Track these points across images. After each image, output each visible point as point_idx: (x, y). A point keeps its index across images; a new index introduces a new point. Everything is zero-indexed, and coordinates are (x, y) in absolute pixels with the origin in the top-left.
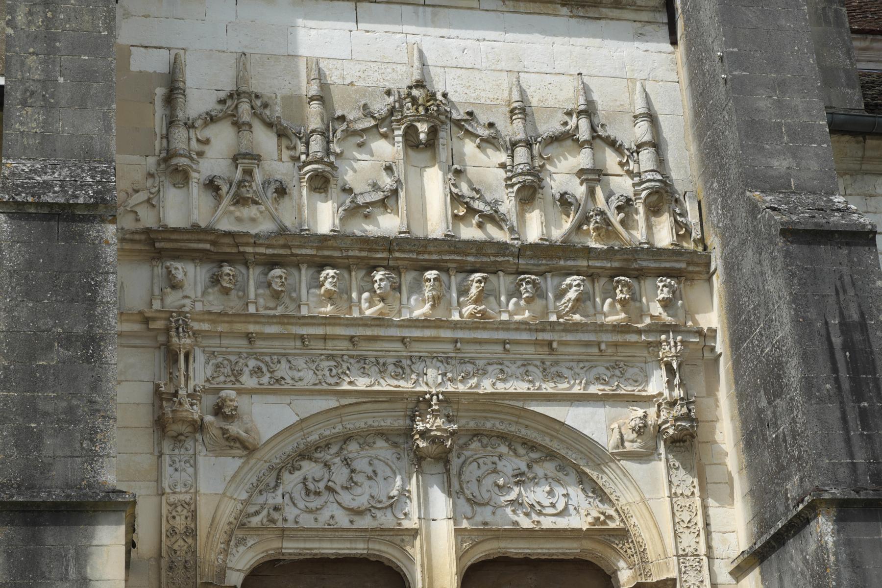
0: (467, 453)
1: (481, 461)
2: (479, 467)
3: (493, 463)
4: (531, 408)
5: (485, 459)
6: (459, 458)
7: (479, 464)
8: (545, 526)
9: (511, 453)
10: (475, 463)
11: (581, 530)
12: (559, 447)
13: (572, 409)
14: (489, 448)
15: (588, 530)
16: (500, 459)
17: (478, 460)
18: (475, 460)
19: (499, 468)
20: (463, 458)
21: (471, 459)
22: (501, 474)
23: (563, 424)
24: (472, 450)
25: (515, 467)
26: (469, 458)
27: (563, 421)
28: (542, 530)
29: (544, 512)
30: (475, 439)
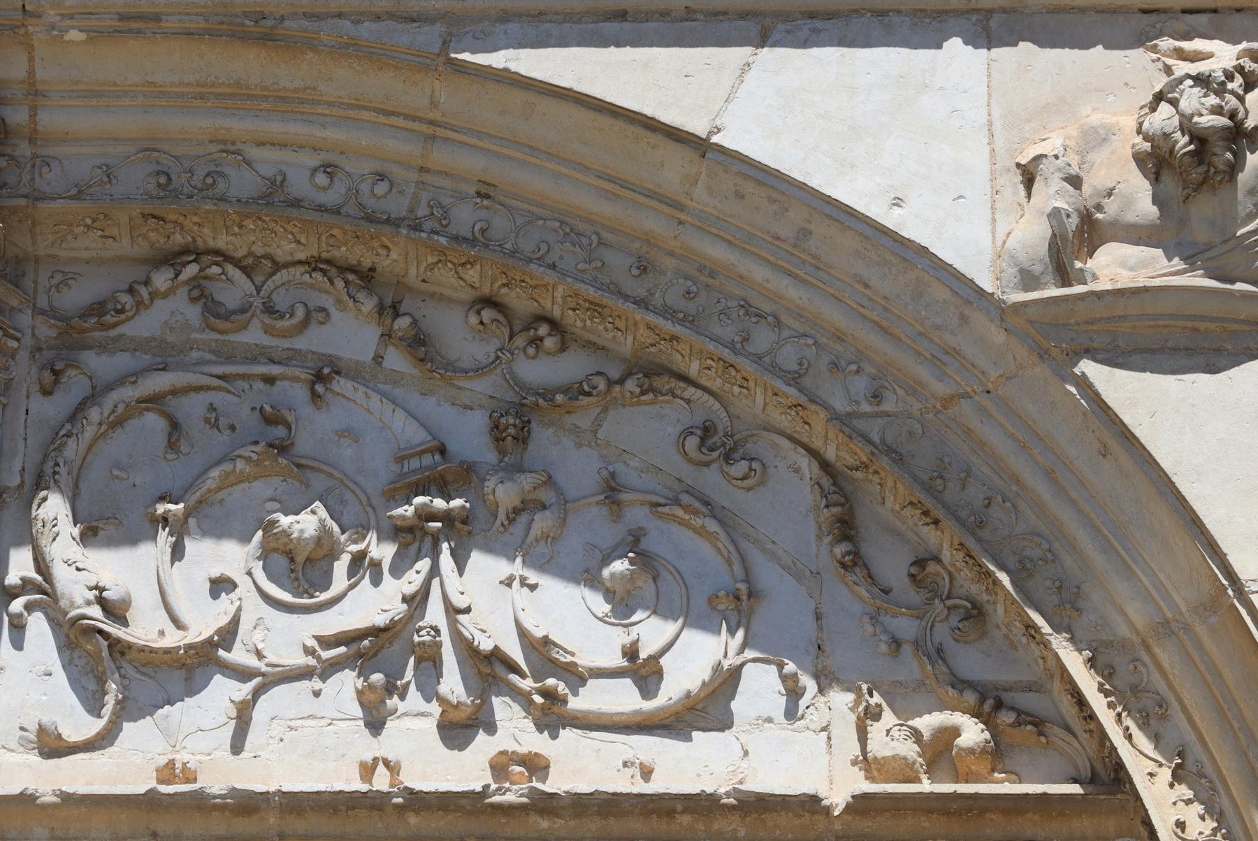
0: (100, 364)
1: (192, 408)
2: (172, 445)
3: (271, 420)
4: (498, 59)
5: (217, 398)
6: (46, 392)
7: (175, 425)
8: (555, 784)
9: (396, 360)
10: (153, 422)
11: (811, 803)
12: (692, 307)
13: (769, 56)
14: (254, 335)
15: (861, 805)
16: (315, 396)
17: (172, 403)
18: (153, 401)
19: (304, 444)
20: (75, 387)
21: (129, 393)
22: (318, 482)
23: (699, 146)
24: (138, 346)
25: (415, 435)
26: (110, 387)
27: (699, 128)
28: (545, 804)
29: (578, 703)
30: (161, 279)
